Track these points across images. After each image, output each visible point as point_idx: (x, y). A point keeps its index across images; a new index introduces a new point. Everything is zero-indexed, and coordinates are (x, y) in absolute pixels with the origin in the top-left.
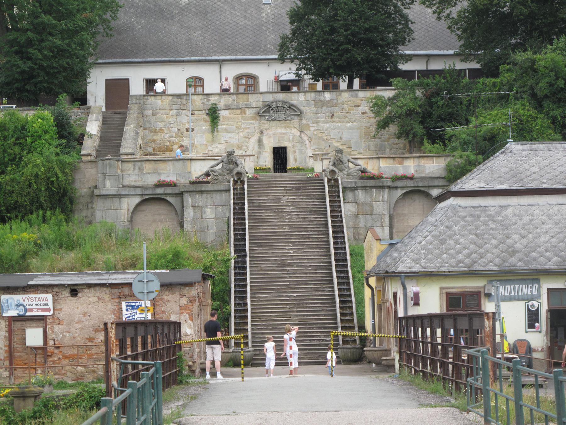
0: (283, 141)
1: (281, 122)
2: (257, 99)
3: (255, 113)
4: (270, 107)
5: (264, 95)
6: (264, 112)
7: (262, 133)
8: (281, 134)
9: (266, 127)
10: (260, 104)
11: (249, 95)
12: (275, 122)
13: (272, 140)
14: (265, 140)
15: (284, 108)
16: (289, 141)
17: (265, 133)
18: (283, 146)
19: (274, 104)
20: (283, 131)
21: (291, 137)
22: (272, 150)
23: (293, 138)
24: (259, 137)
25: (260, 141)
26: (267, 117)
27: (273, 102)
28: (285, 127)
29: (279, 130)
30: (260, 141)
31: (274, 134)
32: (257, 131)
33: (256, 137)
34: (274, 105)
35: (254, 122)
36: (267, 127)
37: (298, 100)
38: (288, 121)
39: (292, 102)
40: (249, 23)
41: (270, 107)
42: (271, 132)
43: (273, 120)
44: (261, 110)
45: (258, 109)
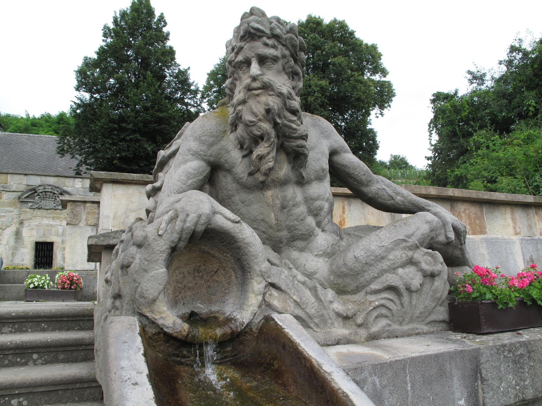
0: (50, 234)
1: (49, 211)
2: (20, 181)
3: (14, 198)
4: (36, 192)
5: (29, 177)
6: (27, 197)
7: (21, 223)
8: (48, 225)
9: (29, 216)
10: (23, 188)
11: (9, 176)
12: (41, 210)
13: (34, 233)
14: (25, 232)
15: (54, 193)
16: (58, 235)
17: (26, 224)
18: (49, 240)
19: (41, 188)
20: (51, 222)
21: (60, 231)
22: (33, 245)
23: (63, 232)
24: (17, 228)
25: (18, 234)
26: (30, 204)
27: (40, 186)
28: (53, 218)
29: (46, 221)
30: (18, 234)
31: (38, 226)
32: (15, 220)
33: (13, 228)
34: (41, 189)
35: (12, 209)
36: (30, 217)
37: (73, 186)
38: (58, 211)
39: (65, 188)
40: (45, 153)
41: (36, 192)
42: (34, 223)
43: (39, 208)
44: (22, 195)
45: (20, 194)
